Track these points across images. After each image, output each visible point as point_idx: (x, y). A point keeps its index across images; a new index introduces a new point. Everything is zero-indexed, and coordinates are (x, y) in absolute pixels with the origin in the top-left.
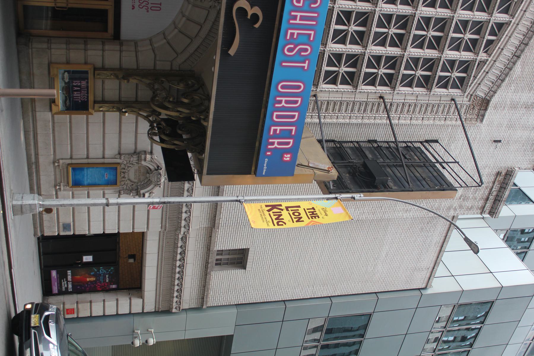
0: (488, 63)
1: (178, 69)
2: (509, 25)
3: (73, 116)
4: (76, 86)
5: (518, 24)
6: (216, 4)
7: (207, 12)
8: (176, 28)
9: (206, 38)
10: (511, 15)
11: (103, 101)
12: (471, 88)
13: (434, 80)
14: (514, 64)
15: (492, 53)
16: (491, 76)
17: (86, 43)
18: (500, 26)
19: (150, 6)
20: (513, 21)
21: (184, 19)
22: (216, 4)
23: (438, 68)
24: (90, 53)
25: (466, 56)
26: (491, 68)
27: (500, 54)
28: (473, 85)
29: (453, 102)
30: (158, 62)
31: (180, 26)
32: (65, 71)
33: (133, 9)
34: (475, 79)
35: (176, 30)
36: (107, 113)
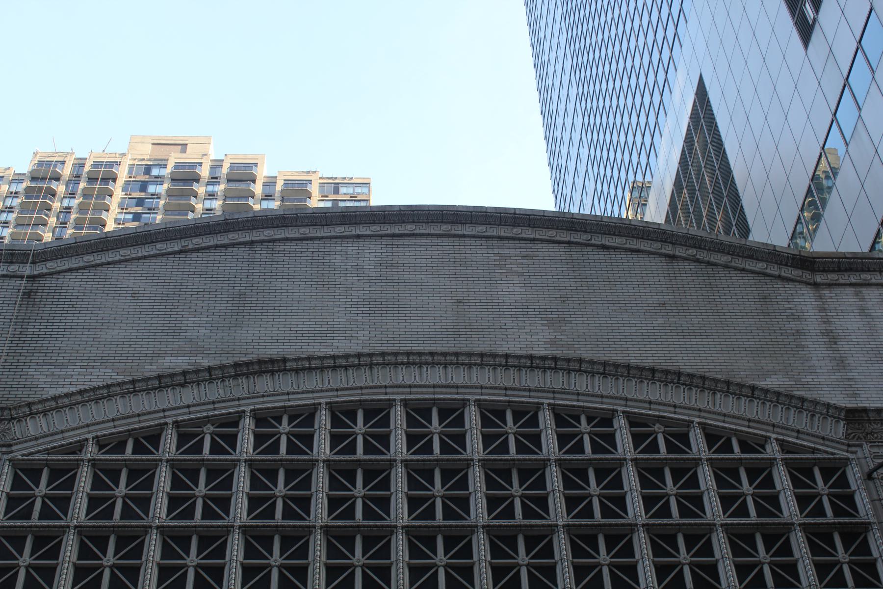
0: (781, 437)
2: (705, 424)
5: (700, 410)
10: (688, 426)
12: (836, 451)
13: (845, 523)
14: (766, 391)
15: (762, 436)
16: (802, 422)
18: (711, 437)
20: (697, 420)
23: (822, 524)
25: (782, 479)
26: (787, 429)
27: (758, 422)
28: (829, 450)
29: (875, 475)
34: (818, 449)
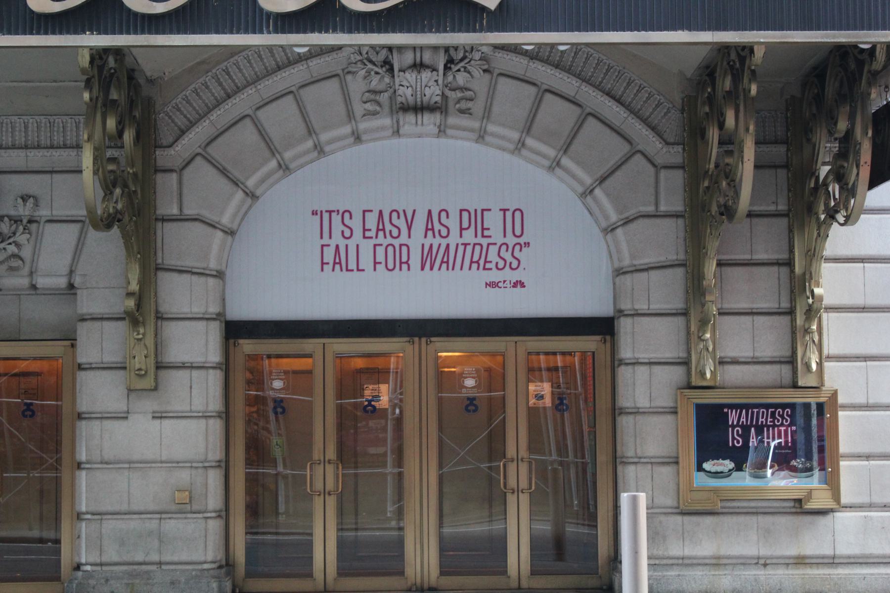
1: (679, 148)
3: (843, 448)
4: (746, 437)
6: (477, 56)
7: (502, 80)
8: (558, 164)
9: (578, 76)
11: (791, 361)
17: (623, 412)
19: (511, 240)
21: (530, 142)
22: (477, 56)
24: (643, 402)
30: (663, 208)
31: (552, 153)
32: (700, 468)
33: (523, 285)
35: (566, 161)
36: (825, 352)
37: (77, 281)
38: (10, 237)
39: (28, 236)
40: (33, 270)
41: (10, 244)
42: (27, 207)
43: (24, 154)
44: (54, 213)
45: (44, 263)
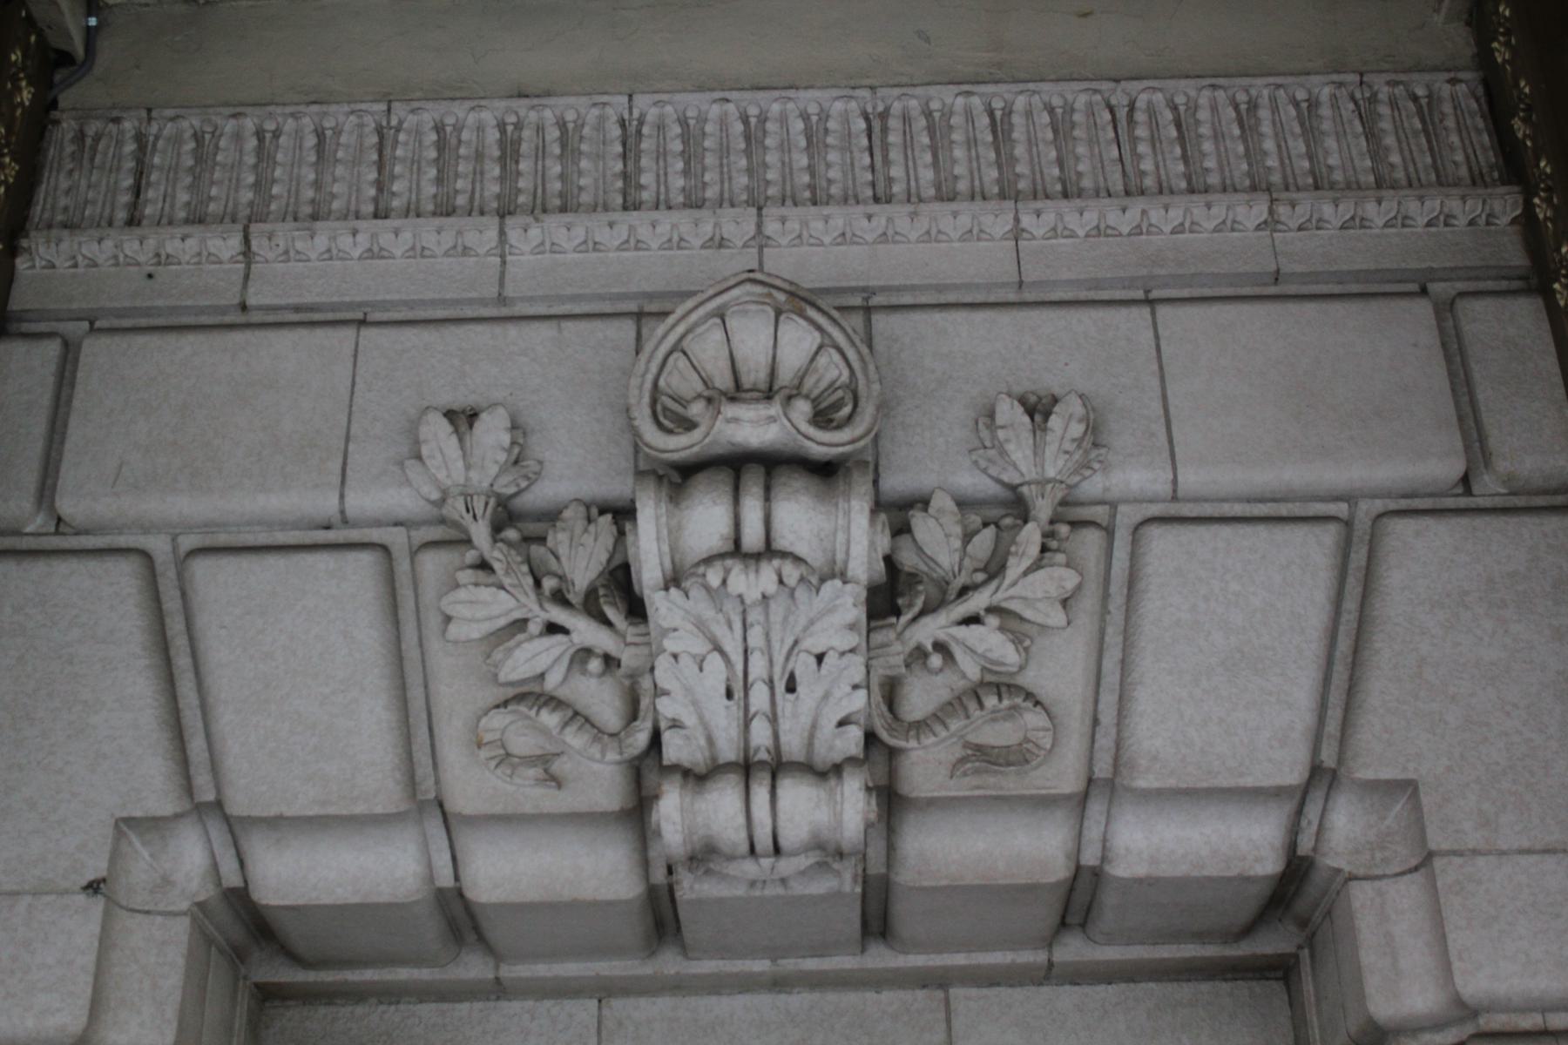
37: (1345, 828)
38: (964, 591)
39: (1070, 579)
40: (1103, 769)
41: (972, 620)
42: (1050, 451)
43: (1003, 225)
44: (1192, 478)
45: (1161, 734)
